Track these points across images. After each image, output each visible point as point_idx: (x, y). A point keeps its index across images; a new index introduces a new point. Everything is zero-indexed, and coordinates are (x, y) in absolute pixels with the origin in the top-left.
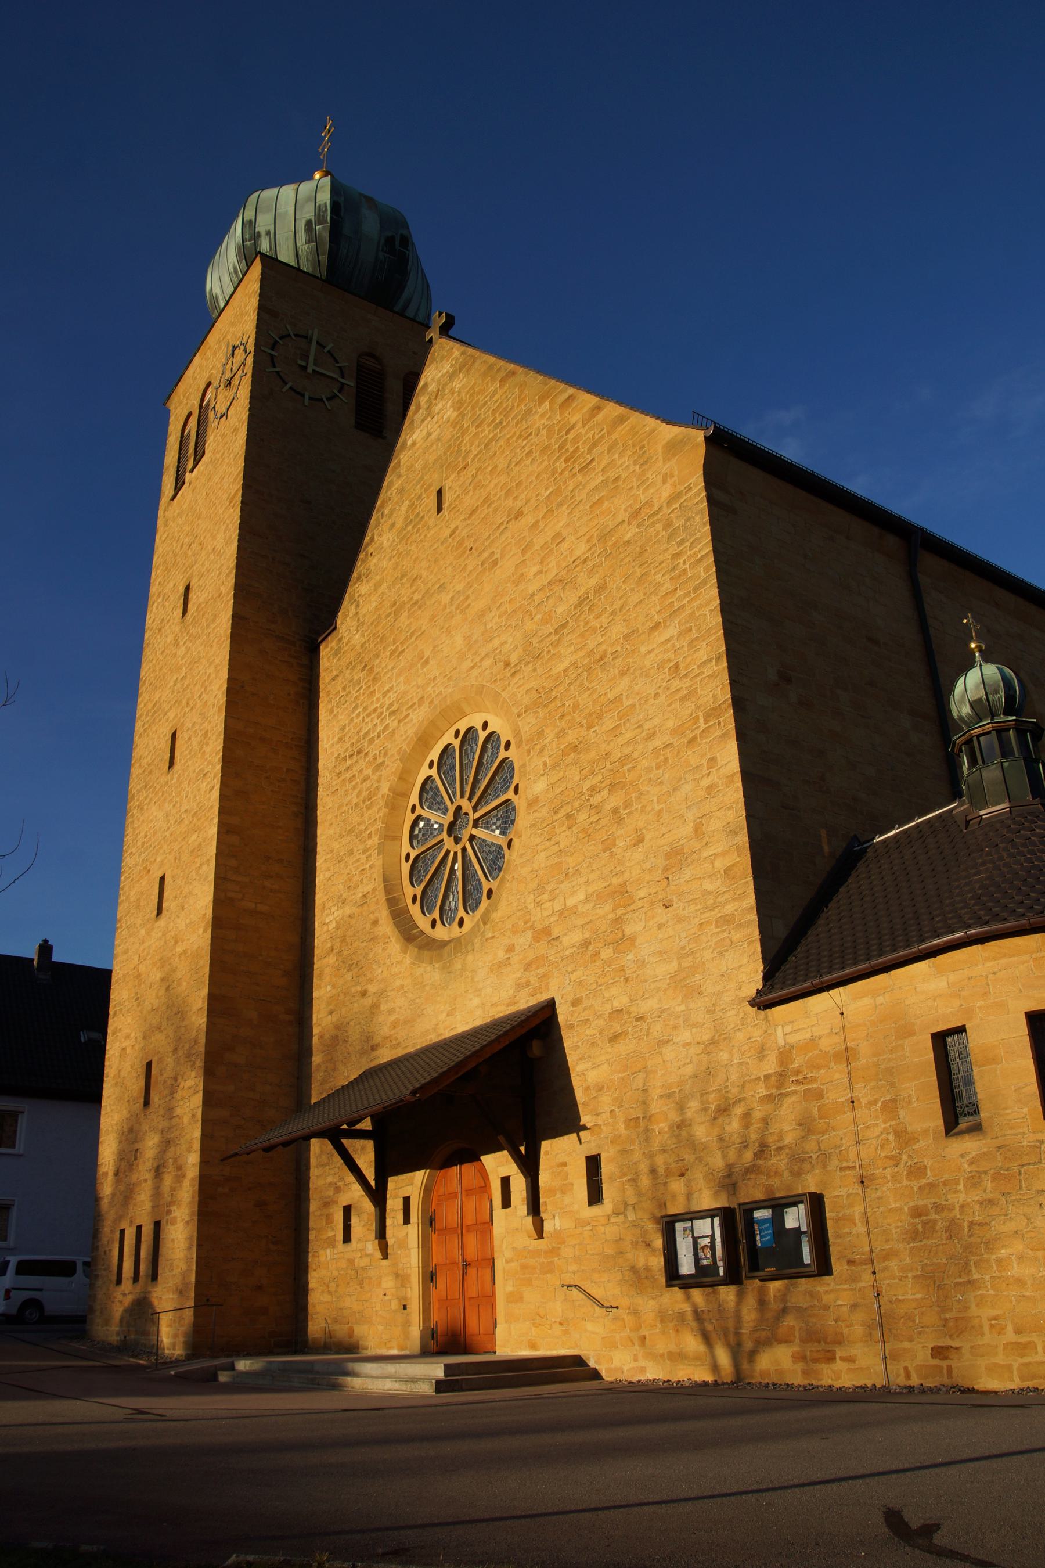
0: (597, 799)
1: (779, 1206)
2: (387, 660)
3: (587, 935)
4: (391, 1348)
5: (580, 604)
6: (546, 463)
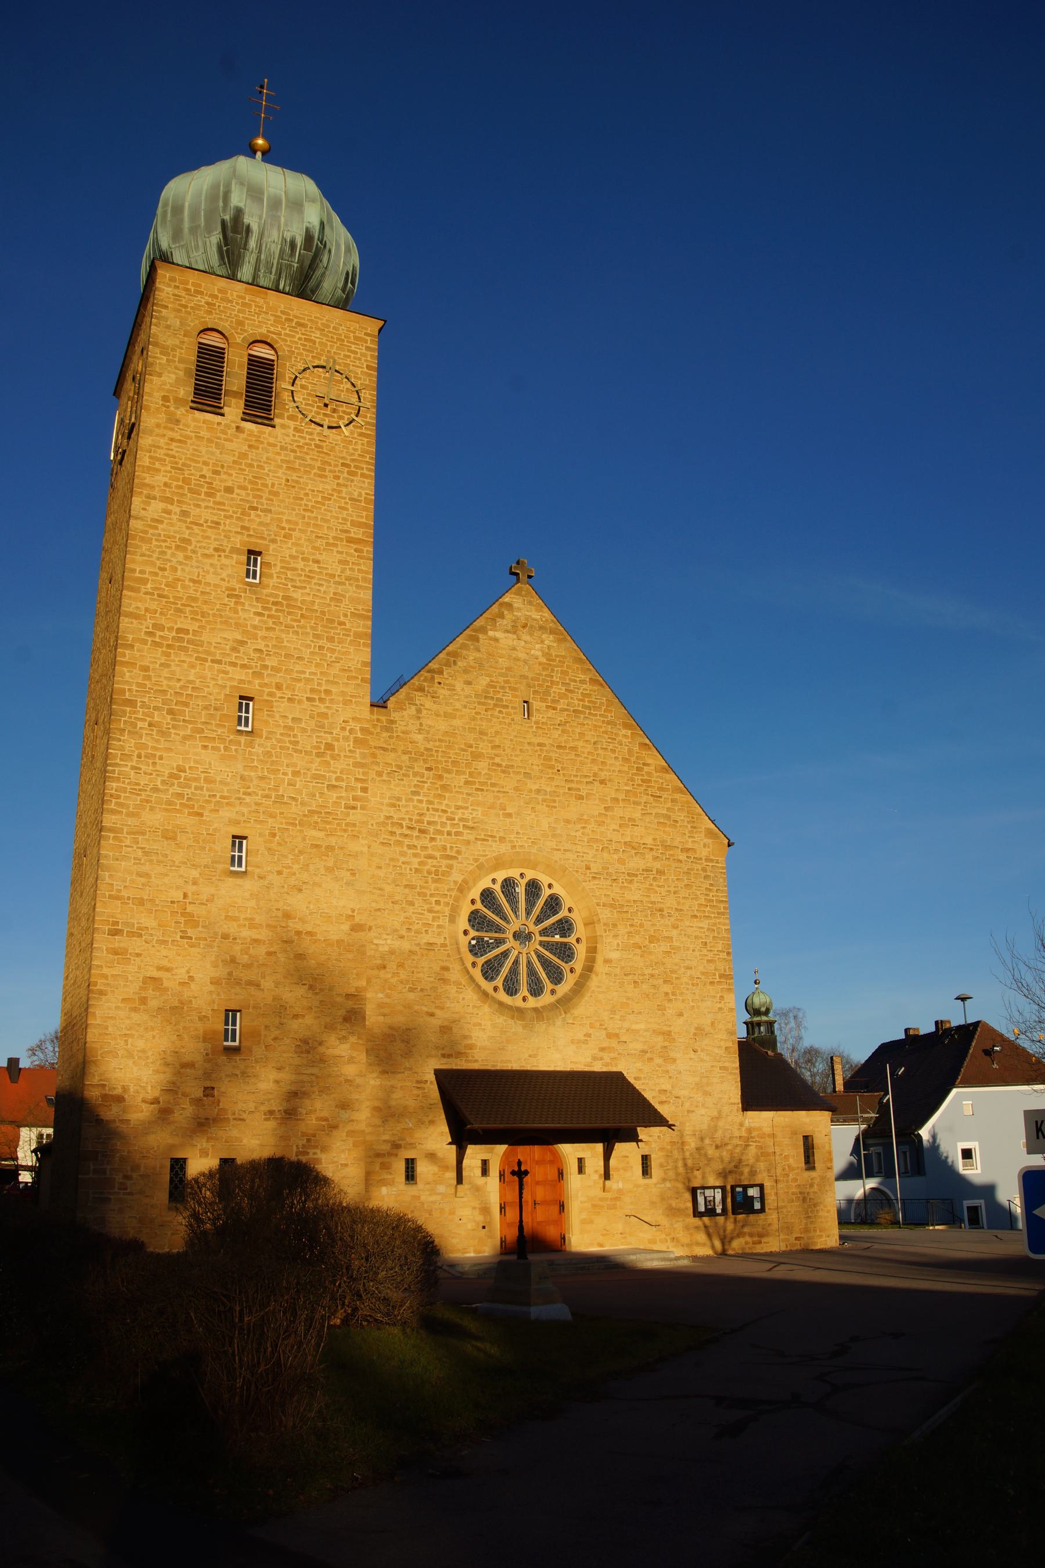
0: (655, 982)
1: (745, 1188)
2: (462, 784)
3: (645, 1048)
4: (470, 1252)
5: (647, 870)
6: (626, 769)
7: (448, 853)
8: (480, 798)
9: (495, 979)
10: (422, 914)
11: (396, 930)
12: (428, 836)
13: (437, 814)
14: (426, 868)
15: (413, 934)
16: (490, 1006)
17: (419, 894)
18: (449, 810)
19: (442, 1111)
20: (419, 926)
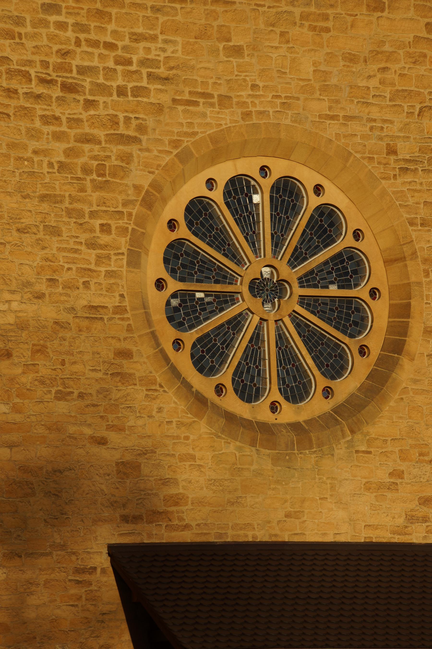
7: (122, 130)
8: (179, 18)
9: (218, 371)
10: (76, 251)
11: (28, 284)
12: (81, 98)
13: (96, 51)
14: (81, 161)
15: (60, 290)
16: (210, 423)
17: (69, 213)
18: (120, 44)
19: (125, 626)
20: (72, 274)
